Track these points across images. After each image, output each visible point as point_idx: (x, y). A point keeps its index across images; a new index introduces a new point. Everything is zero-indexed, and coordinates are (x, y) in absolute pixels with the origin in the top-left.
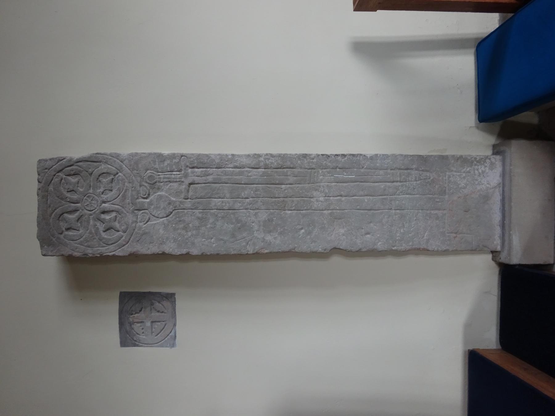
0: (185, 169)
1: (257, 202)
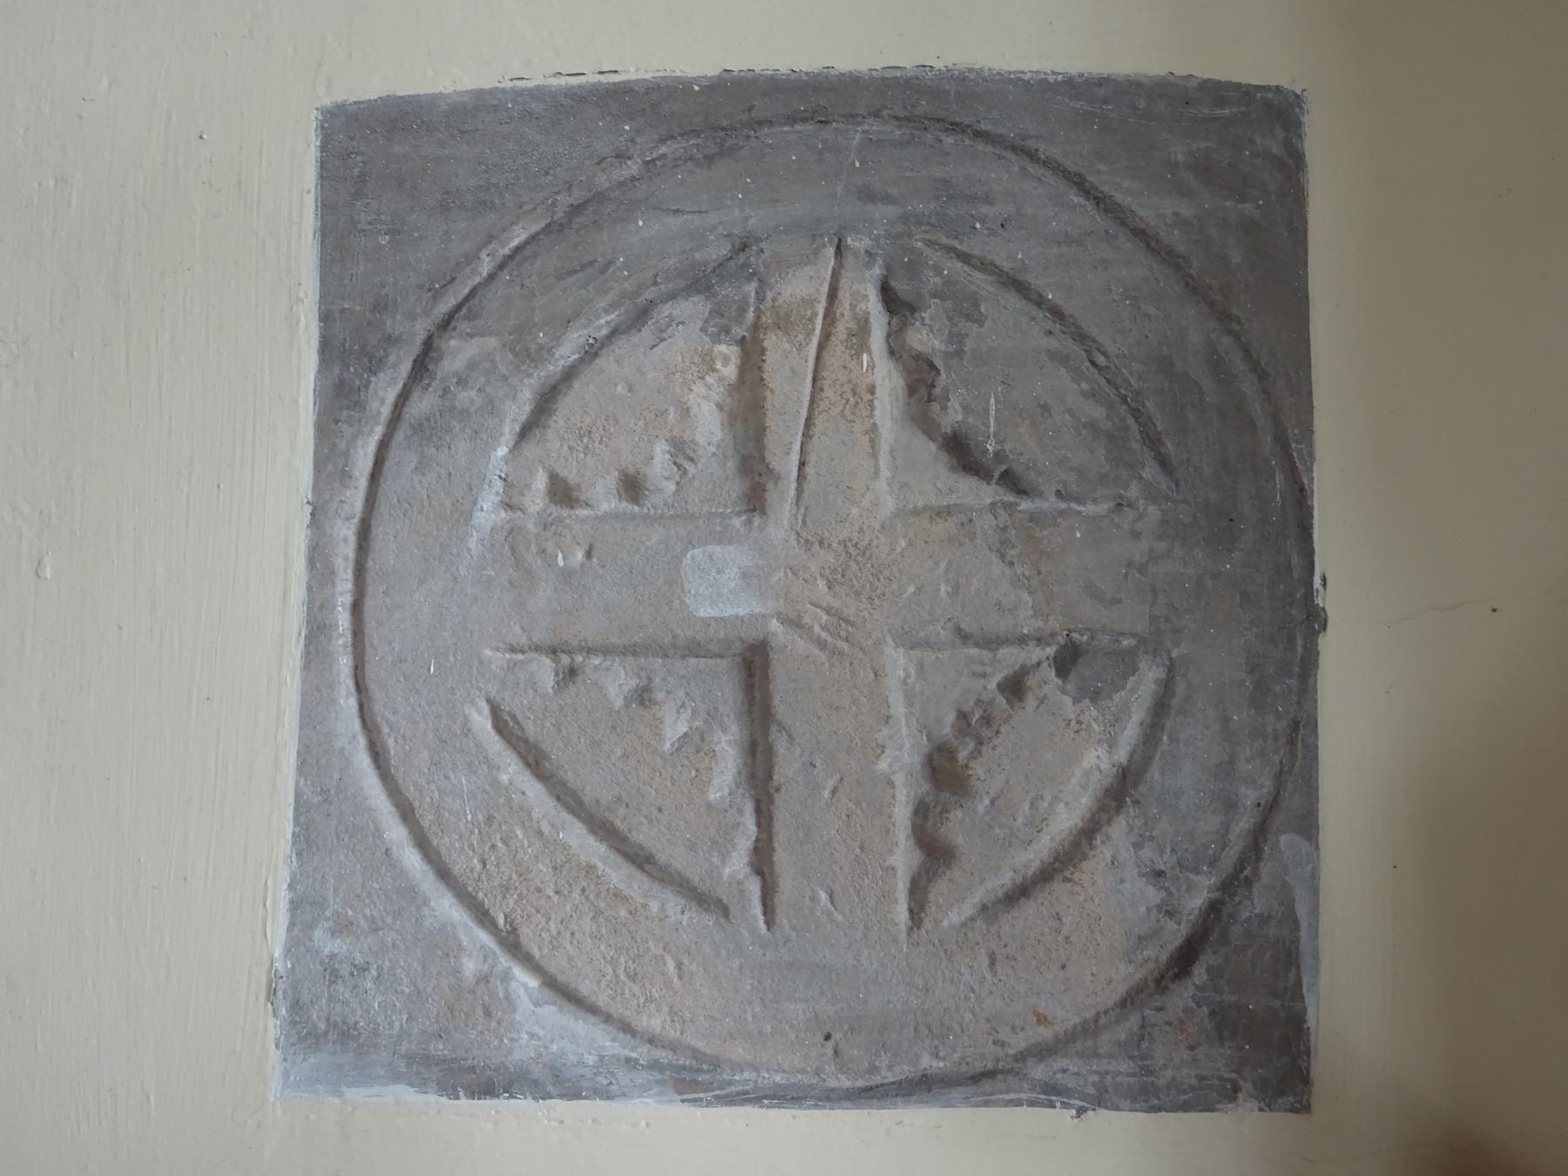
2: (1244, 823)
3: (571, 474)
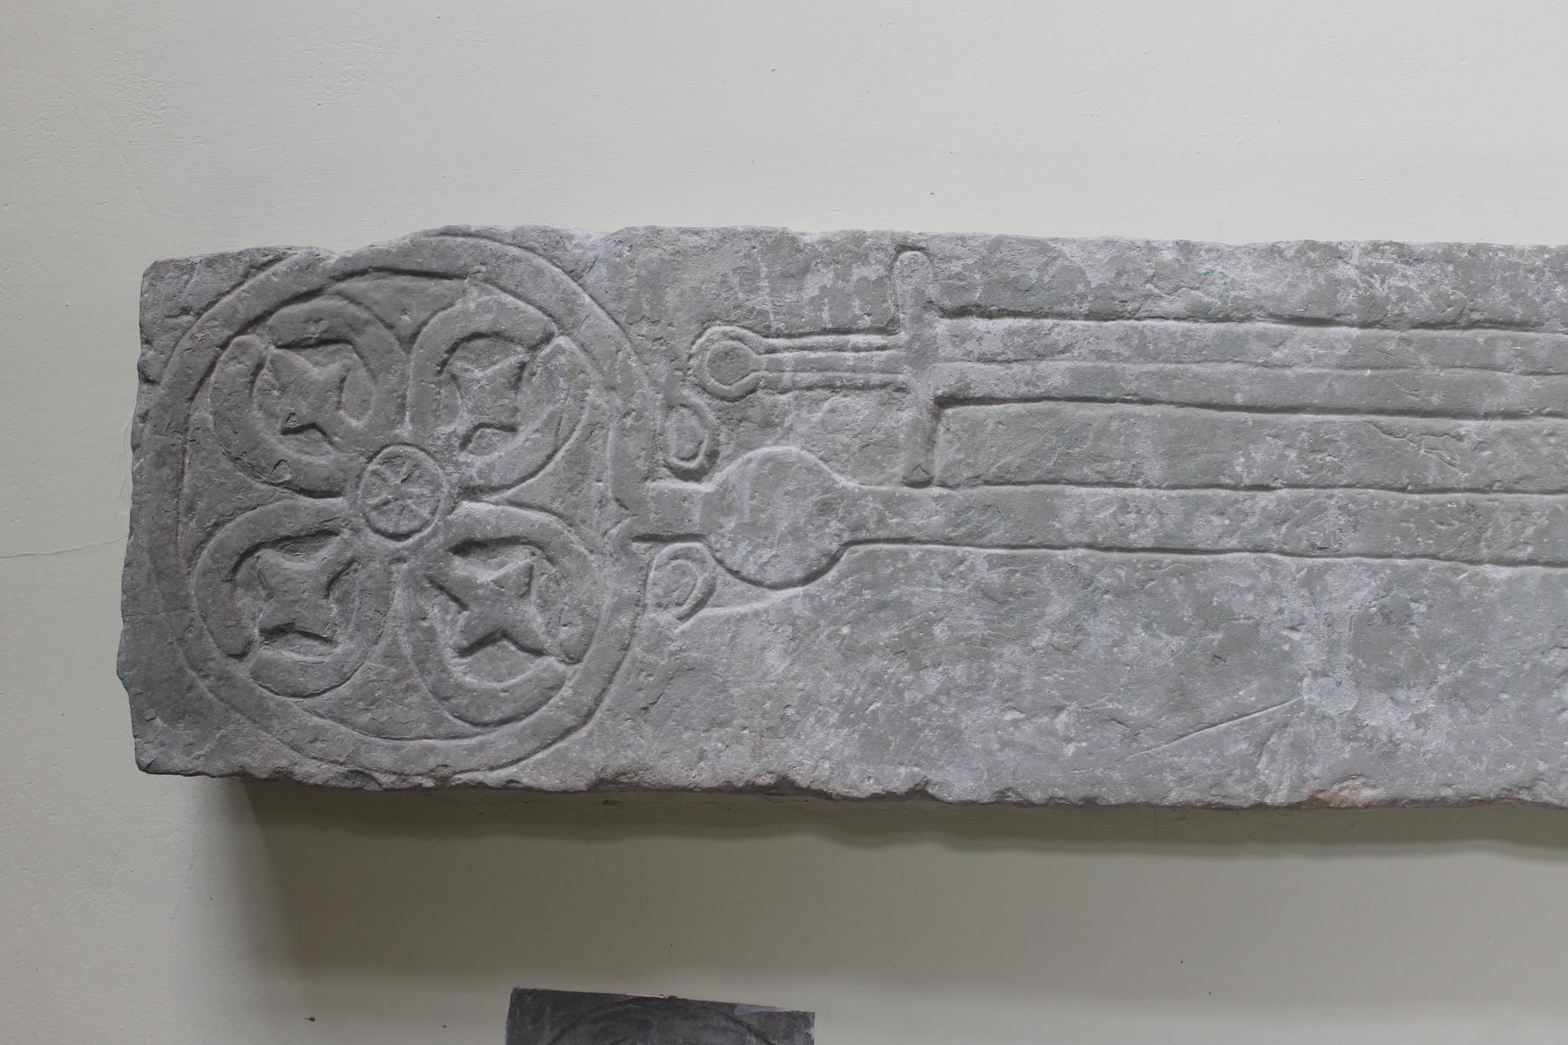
0: (918, 319)
1: (1320, 509)
2: (731, 1025)
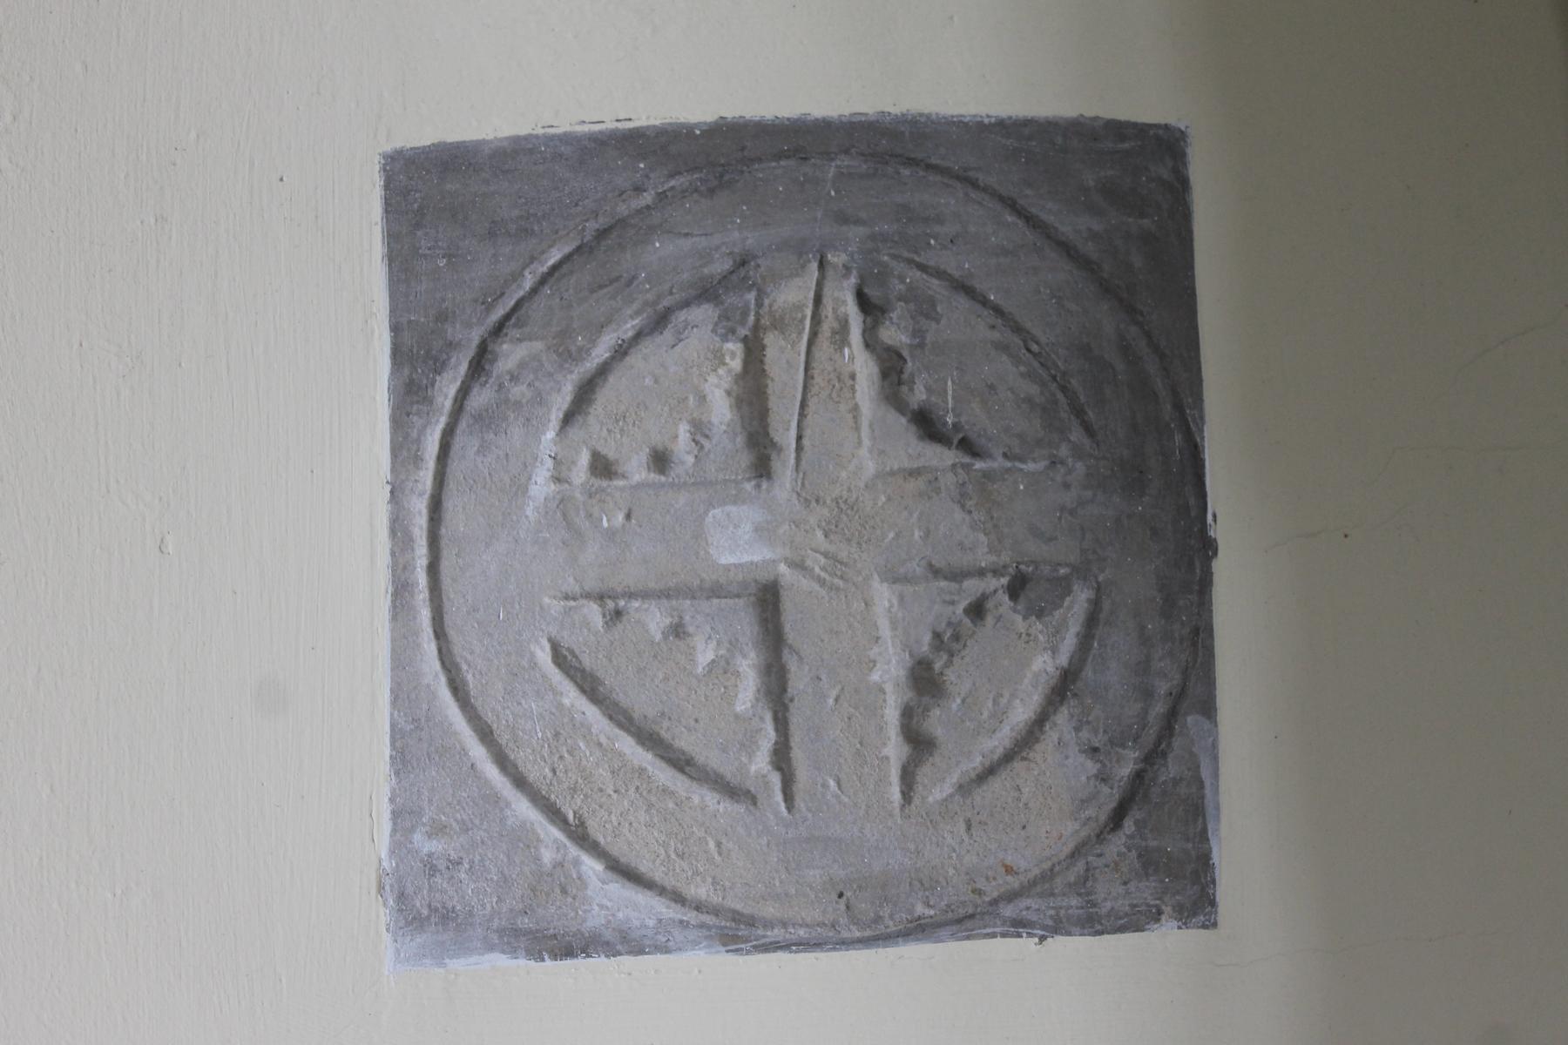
2: (1159, 708)
3: (610, 452)
